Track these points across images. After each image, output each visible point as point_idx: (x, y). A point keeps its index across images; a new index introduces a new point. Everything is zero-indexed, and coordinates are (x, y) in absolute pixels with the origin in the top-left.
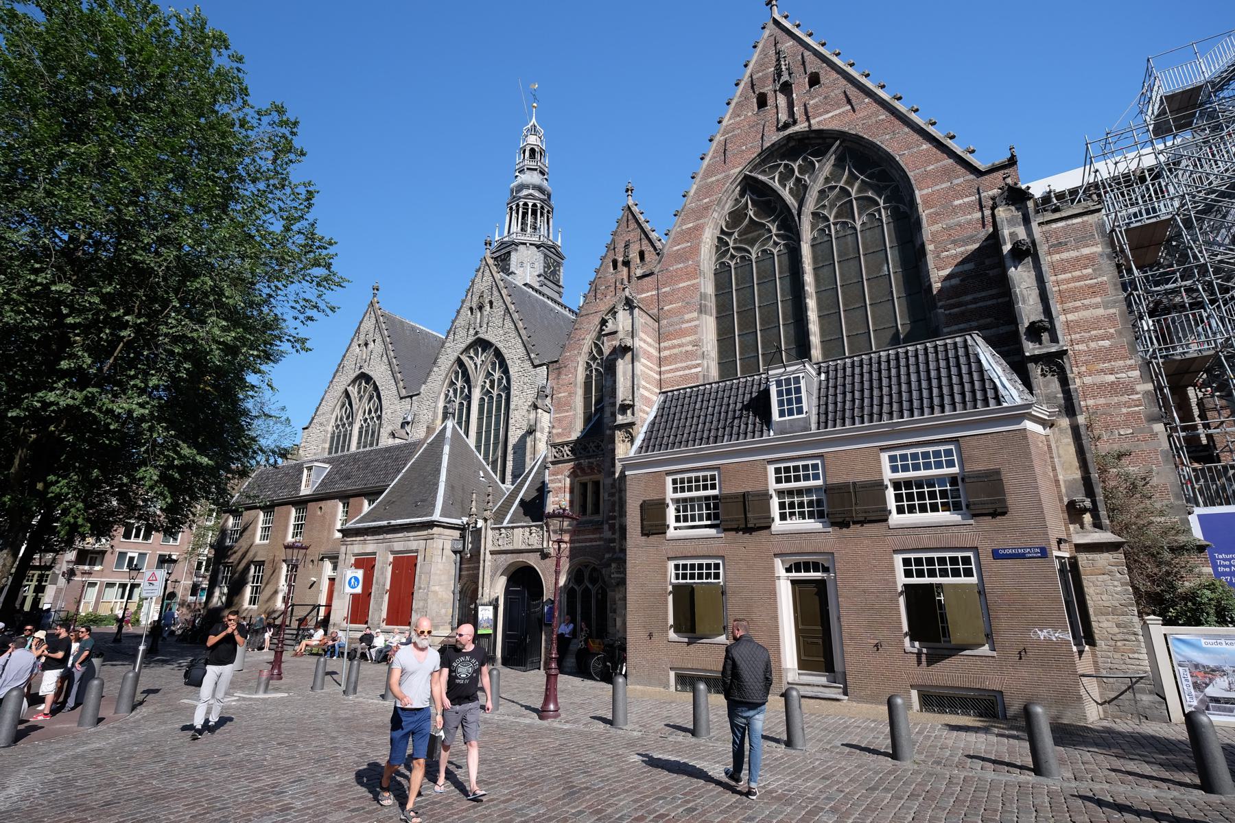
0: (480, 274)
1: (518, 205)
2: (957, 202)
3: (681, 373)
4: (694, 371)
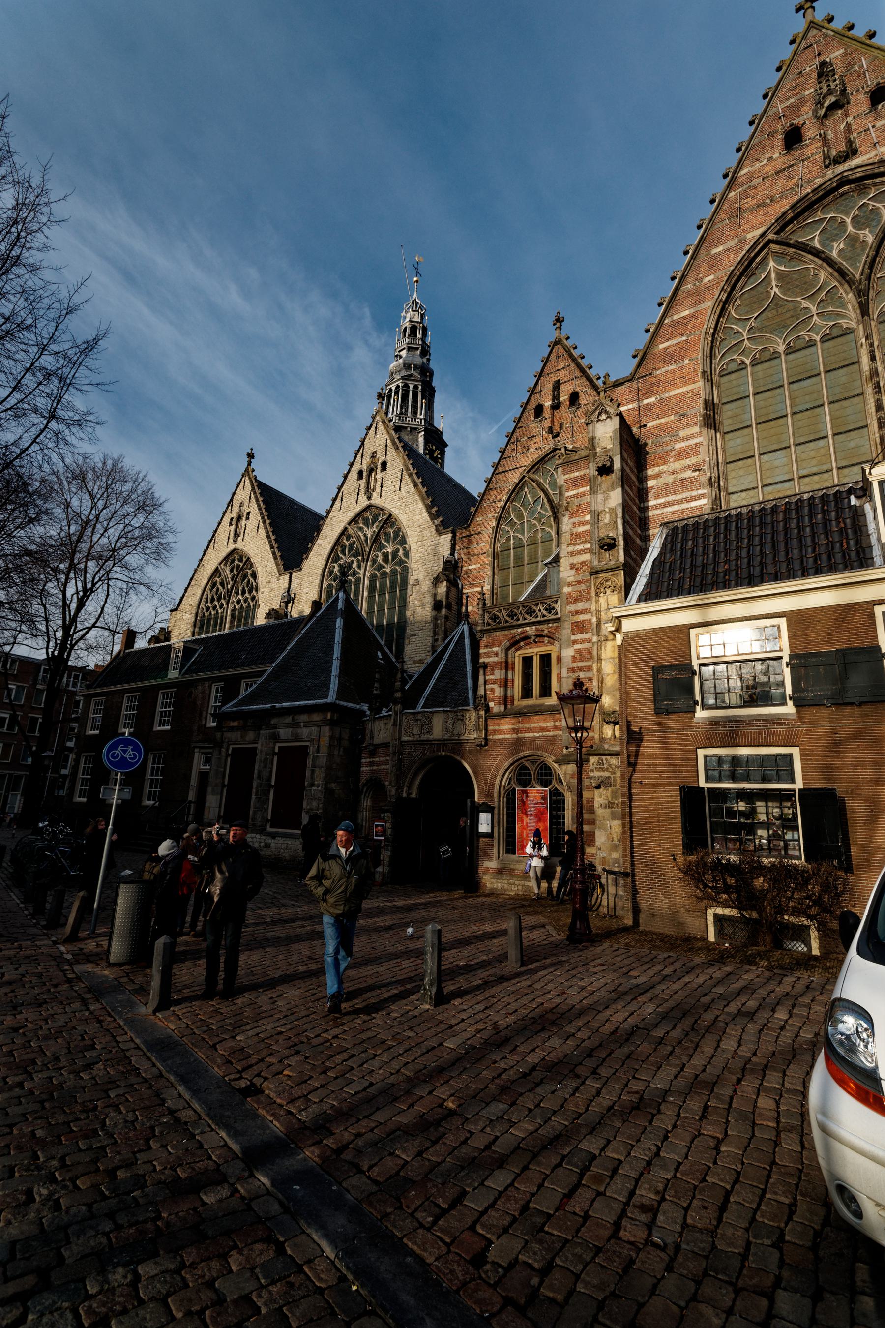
0: (372, 431)
1: (398, 386)
3: (675, 508)
4: (694, 504)
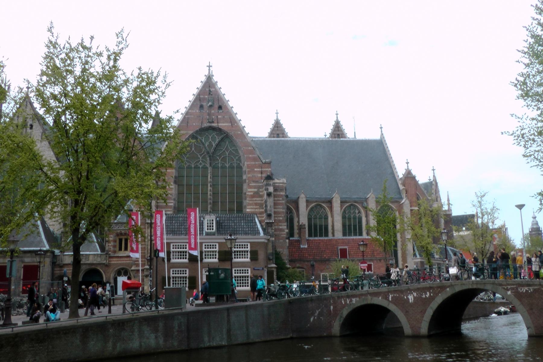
2: (256, 169)
